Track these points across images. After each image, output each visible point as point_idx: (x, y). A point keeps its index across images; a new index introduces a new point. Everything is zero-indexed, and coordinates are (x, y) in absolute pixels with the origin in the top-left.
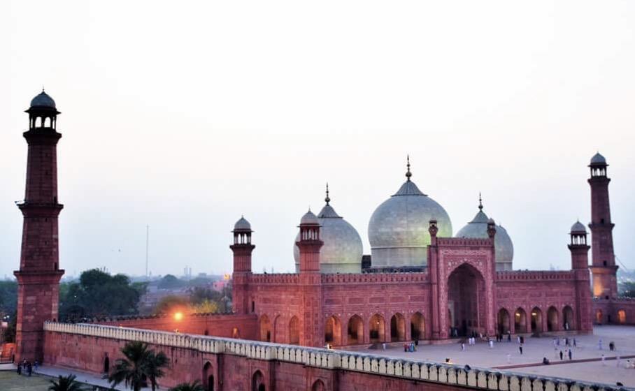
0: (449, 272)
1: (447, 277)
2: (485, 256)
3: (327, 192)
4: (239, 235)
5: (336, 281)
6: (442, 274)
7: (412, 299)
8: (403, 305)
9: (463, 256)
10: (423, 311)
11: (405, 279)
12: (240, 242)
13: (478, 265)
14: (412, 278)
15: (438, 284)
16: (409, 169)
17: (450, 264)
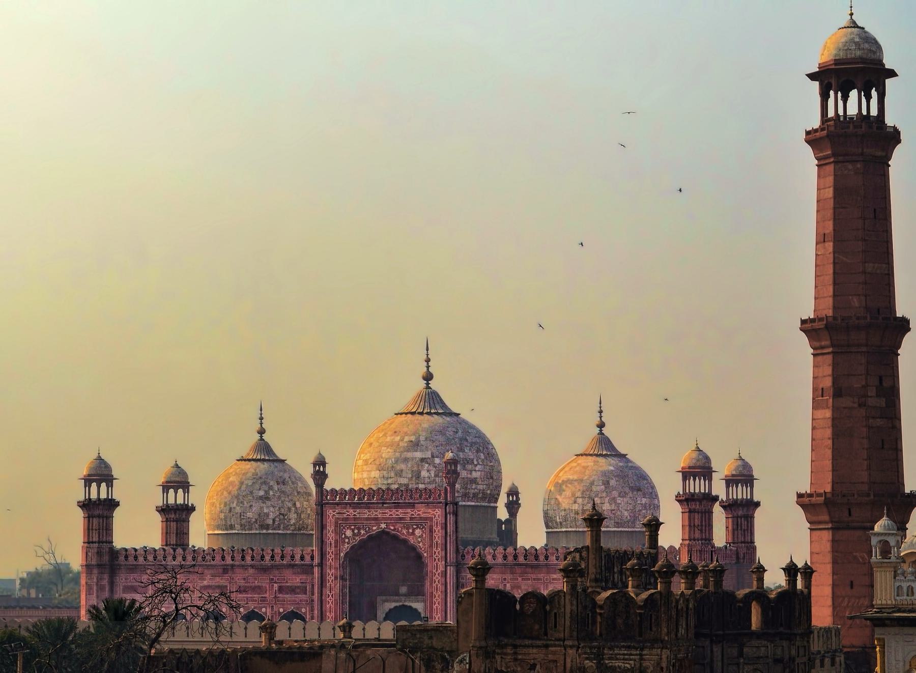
0: (346, 547)
1: (342, 555)
2: (431, 519)
3: (261, 419)
4: (171, 491)
5: (141, 559)
6: (330, 550)
7: (281, 589)
8: (264, 600)
9: (376, 519)
10: (303, 610)
11: (268, 558)
12: (171, 501)
13: (413, 533)
14: (282, 557)
15: (321, 565)
16: (428, 367)
17: (349, 533)
